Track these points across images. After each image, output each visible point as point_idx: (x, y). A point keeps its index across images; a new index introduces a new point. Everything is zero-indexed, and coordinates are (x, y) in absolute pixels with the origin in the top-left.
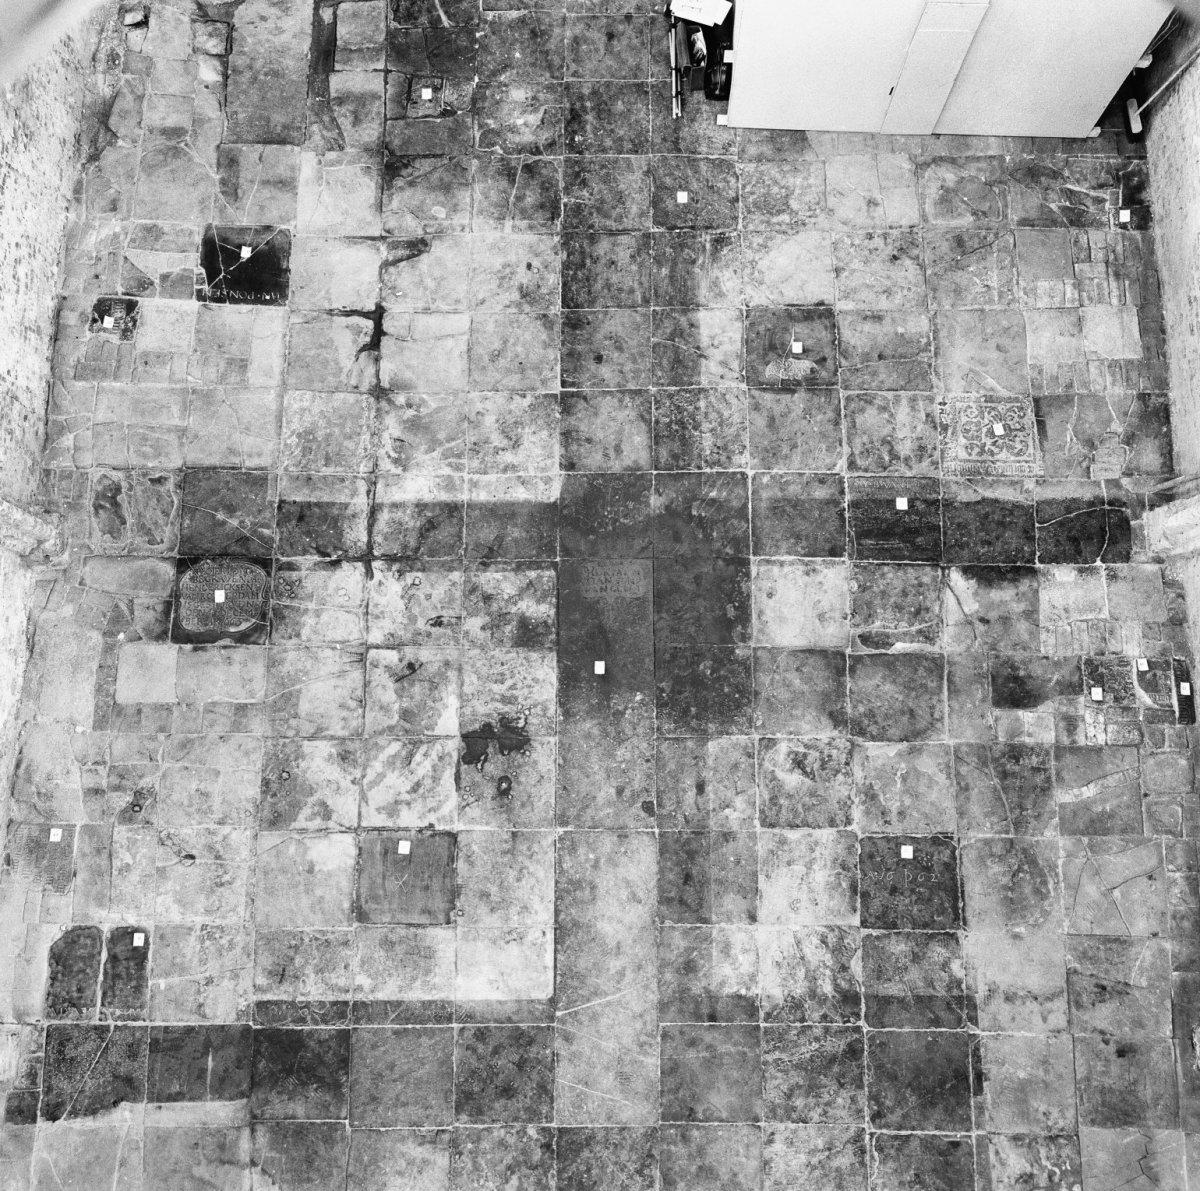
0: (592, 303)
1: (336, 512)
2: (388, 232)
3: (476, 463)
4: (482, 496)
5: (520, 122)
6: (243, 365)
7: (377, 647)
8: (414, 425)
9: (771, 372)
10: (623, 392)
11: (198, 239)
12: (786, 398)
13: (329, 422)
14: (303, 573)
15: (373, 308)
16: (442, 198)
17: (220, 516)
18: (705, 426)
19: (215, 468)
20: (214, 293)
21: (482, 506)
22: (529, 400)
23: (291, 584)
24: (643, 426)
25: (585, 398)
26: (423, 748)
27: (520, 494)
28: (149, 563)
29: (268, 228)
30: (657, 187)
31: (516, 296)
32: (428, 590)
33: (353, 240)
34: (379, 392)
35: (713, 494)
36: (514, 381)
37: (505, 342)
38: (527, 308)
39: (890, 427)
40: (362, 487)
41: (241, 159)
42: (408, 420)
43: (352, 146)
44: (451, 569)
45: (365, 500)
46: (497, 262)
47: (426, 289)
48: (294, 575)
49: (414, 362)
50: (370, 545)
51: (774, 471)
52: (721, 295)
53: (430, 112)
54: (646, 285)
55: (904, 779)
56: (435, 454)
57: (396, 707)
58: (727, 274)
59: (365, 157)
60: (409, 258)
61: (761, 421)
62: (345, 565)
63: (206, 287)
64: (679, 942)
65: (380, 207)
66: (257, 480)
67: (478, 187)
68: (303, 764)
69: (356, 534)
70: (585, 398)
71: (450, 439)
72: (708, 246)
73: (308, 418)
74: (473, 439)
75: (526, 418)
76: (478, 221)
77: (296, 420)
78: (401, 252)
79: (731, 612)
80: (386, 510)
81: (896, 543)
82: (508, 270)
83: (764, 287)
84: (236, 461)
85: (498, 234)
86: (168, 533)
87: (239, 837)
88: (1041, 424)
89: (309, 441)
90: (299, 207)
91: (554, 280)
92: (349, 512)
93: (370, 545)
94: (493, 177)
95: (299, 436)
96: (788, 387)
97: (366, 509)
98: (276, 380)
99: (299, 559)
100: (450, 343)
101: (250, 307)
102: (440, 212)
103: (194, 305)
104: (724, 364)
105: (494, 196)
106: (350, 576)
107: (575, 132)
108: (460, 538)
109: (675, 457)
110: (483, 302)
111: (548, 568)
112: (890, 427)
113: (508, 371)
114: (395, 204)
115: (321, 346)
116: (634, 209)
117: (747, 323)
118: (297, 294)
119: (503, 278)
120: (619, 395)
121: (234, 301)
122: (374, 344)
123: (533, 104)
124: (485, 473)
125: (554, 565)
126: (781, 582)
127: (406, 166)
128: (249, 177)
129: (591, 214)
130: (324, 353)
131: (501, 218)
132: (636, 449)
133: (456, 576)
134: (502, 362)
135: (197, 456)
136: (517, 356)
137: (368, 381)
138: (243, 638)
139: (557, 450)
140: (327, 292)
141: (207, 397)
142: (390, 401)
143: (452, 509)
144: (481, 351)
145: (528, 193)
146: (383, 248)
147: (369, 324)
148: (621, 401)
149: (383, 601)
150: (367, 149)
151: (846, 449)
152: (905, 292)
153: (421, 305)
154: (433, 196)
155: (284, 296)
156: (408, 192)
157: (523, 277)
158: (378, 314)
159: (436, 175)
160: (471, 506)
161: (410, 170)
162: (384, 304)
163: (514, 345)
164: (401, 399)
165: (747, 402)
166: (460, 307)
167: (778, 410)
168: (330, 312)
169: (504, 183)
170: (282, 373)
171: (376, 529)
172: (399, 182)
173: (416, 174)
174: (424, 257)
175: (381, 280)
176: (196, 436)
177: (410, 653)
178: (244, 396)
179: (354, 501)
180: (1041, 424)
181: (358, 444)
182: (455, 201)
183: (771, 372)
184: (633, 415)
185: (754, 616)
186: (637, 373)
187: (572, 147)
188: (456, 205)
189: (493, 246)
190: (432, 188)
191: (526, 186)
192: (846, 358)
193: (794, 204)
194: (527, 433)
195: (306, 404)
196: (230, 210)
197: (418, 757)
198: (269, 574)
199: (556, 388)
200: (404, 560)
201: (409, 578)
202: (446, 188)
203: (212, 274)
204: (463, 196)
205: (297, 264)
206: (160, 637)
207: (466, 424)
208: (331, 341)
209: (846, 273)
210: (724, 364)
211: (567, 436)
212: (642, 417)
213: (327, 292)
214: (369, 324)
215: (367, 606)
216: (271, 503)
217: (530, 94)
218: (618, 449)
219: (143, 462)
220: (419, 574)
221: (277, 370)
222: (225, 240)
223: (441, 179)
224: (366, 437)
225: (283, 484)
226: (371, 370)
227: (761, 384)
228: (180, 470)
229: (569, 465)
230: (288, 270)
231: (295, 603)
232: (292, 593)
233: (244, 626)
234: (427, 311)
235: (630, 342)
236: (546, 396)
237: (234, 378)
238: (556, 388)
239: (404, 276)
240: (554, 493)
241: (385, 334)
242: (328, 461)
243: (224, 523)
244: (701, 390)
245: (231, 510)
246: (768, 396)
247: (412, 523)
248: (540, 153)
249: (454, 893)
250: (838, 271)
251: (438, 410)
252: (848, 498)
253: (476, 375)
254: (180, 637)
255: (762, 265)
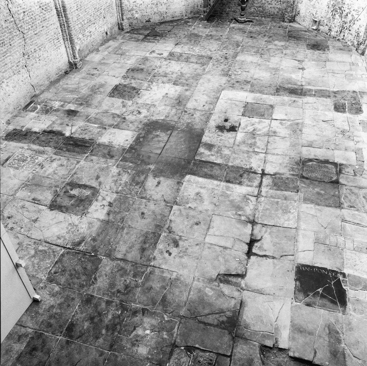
0: (147, 233)
1: (275, 188)
2: (239, 290)
3: (216, 192)
4: (216, 182)
5: (148, 332)
6: (317, 241)
7: (262, 153)
8: (239, 208)
9: (87, 193)
10: (149, 199)
11: (349, 305)
12: (88, 184)
13: (276, 215)
14: (288, 173)
15: (252, 257)
16: (205, 298)
17: (323, 192)
18: (122, 182)
19: (327, 206)
20: (336, 274)
21: (217, 179)
22: (188, 206)
23: (293, 171)
24: (146, 187)
25: (165, 201)
26: (250, 131)
27: (201, 180)
28: (351, 184)
29: (308, 305)
30: (91, 276)
31: (181, 243)
32: (241, 163)
33: (260, 292)
34: (253, 223)
35: (131, 164)
36: (192, 213)
37: (191, 227)
38: (177, 238)
39: (58, 169)
40: (263, 193)
41: (328, 354)
42: (241, 211)
43: (254, 345)
44: (232, 166)
45: (262, 190)
46: (185, 260)
47: (224, 258)
48: (292, 173)
49: (235, 230)
50: (262, 177)
51: (106, 165)
52: (90, 223)
53: (201, 354)
54: (119, 235)
55: (113, 107)
56: (232, 198)
57: (257, 140)
58: (81, 231)
59: (247, 335)
60: (230, 275)
61: (101, 179)
62: (272, 173)
63: (341, 278)
64: (188, 93)
65: (242, 303)
66: (306, 200)
67: (185, 299)
68: (289, 133)
69: (266, 181)
70: (165, 201)
71: (225, 201)
72: (83, 244)
73: (286, 218)
74: (215, 199)
75: (191, 201)
76: (189, 281)
77: (291, 217)
78: (234, 280)
79: (141, 140)
80: (255, 185)
81: (80, 143)
82: (181, 255)
83: (71, 222)
84: (317, 207)
85: (181, 272)
86: (344, 191)
87: (307, 121)
88: (7, 160)
89: (285, 210)
90: (289, 313)
91: (161, 246)
92: (269, 187)
93: (262, 177)
94: (174, 301)
95: (290, 212)
96: (85, 187)
97: (262, 187)
98: (301, 232)
99: (289, 177)
100: (217, 233)
101: (316, 265)
102: (209, 292)
103: (346, 271)
104: (104, 199)
105: (177, 291)
106: (270, 170)
107: (119, 316)
108: (227, 173)
109: (139, 176)
110: (197, 245)
111: (197, 159)
112: (58, 169)
113: (193, 217)
114: (233, 302)
115: (279, 244)
116: (108, 268)
117: (86, 211)
118: (291, 269)
119: (185, 252)
120: (150, 199)
121: (325, 269)
122: (252, 242)
123: (136, 342)
124: (213, 189)
125: (195, 160)
126: (122, 142)
127: (223, 322)
128: (321, 340)
129: (130, 271)
130: (277, 240)
131: (177, 279)
132: (151, 182)
133: (230, 164)
134: (196, 220)
135: (337, 211)
136: (188, 221)
137: (257, 228)
138: (310, 160)
139: (182, 188)
140: (275, 267)
141: (333, 230)
142: (249, 218)
143: (228, 181)
144: (204, 227)
145: (158, 289)
146: (243, 285)
147: (254, 251)
148: (151, 197)
149: (259, 163)
150: (246, 340)
151: (77, 166)
152: (16, 205)
153: (228, 251)
154: (211, 301)
155: (298, 267)
156: (225, 306)
157: (174, 251)
158: (249, 253)
159: (207, 311)
160: (221, 181)
161: (221, 319)
162: (246, 257)
163: (188, 225)
164: (243, 218)
165: (103, 186)
166: (209, 246)
167: (93, 181)
168: (274, 258)
169: (169, 297)
170: (298, 235)
171: (259, 181)
172: (229, 314)
173: (217, 316)
174: (222, 272)
175: (246, 269)
176: (337, 217)
177: (251, 150)
178: (316, 229)
179: (267, 190)
180: (7, 160)
181: (264, 207)
182: (199, 294)
183: (87, 193)
184: (148, 192)
185: (135, 138)
186: (140, 204)
187: (124, 308)
188: (199, 292)
189: (184, 267)
190: (210, 305)
191: (157, 293)
192: (57, 191)
193: (33, 252)
194: (192, 196)
195: (287, 222)
196: (333, 321)
197: (251, 130)
198: (302, 174)
199: (175, 207)
200: (250, 171)
201: (248, 167)
202: (202, 301)
203: (338, 284)
204: (193, 295)
205: (291, 284)
206: (341, 165)
207: (217, 204)
208: (274, 245)
209: (33, 218)
210: (104, 199)
211: (178, 190)
212: (145, 190)
213: (275, 267)
214: (254, 251)
215: (264, 162)
216: (301, 192)
217: (135, 349)
218: (159, 183)
219: (360, 214)
220: (244, 167)
221: (301, 236)
222: (335, 303)
223: (204, 308)
224: (261, 208)
225: (296, 198)
226: (255, 232)
227: (94, 190)
228: (342, 208)
229: (179, 183)
230: (296, 280)
231: (291, 166)
232: (292, 169)
233: (311, 163)
234: (225, 248)
235: (137, 215)
236: (180, 205)
237: (322, 236)
238: (175, 207)
239: (234, 267)
240: (188, 177)
241: (247, 244)
242: (277, 203)
243: (321, 190)
244: (117, 193)
245: (318, 193)
246: (94, 185)
247: (245, 180)
248: (143, 309)
249: (245, 107)
250: (35, 221)
251: (228, 211)
252: (86, 155)
253: (209, 219)
254: (335, 164)
255: (65, 231)
